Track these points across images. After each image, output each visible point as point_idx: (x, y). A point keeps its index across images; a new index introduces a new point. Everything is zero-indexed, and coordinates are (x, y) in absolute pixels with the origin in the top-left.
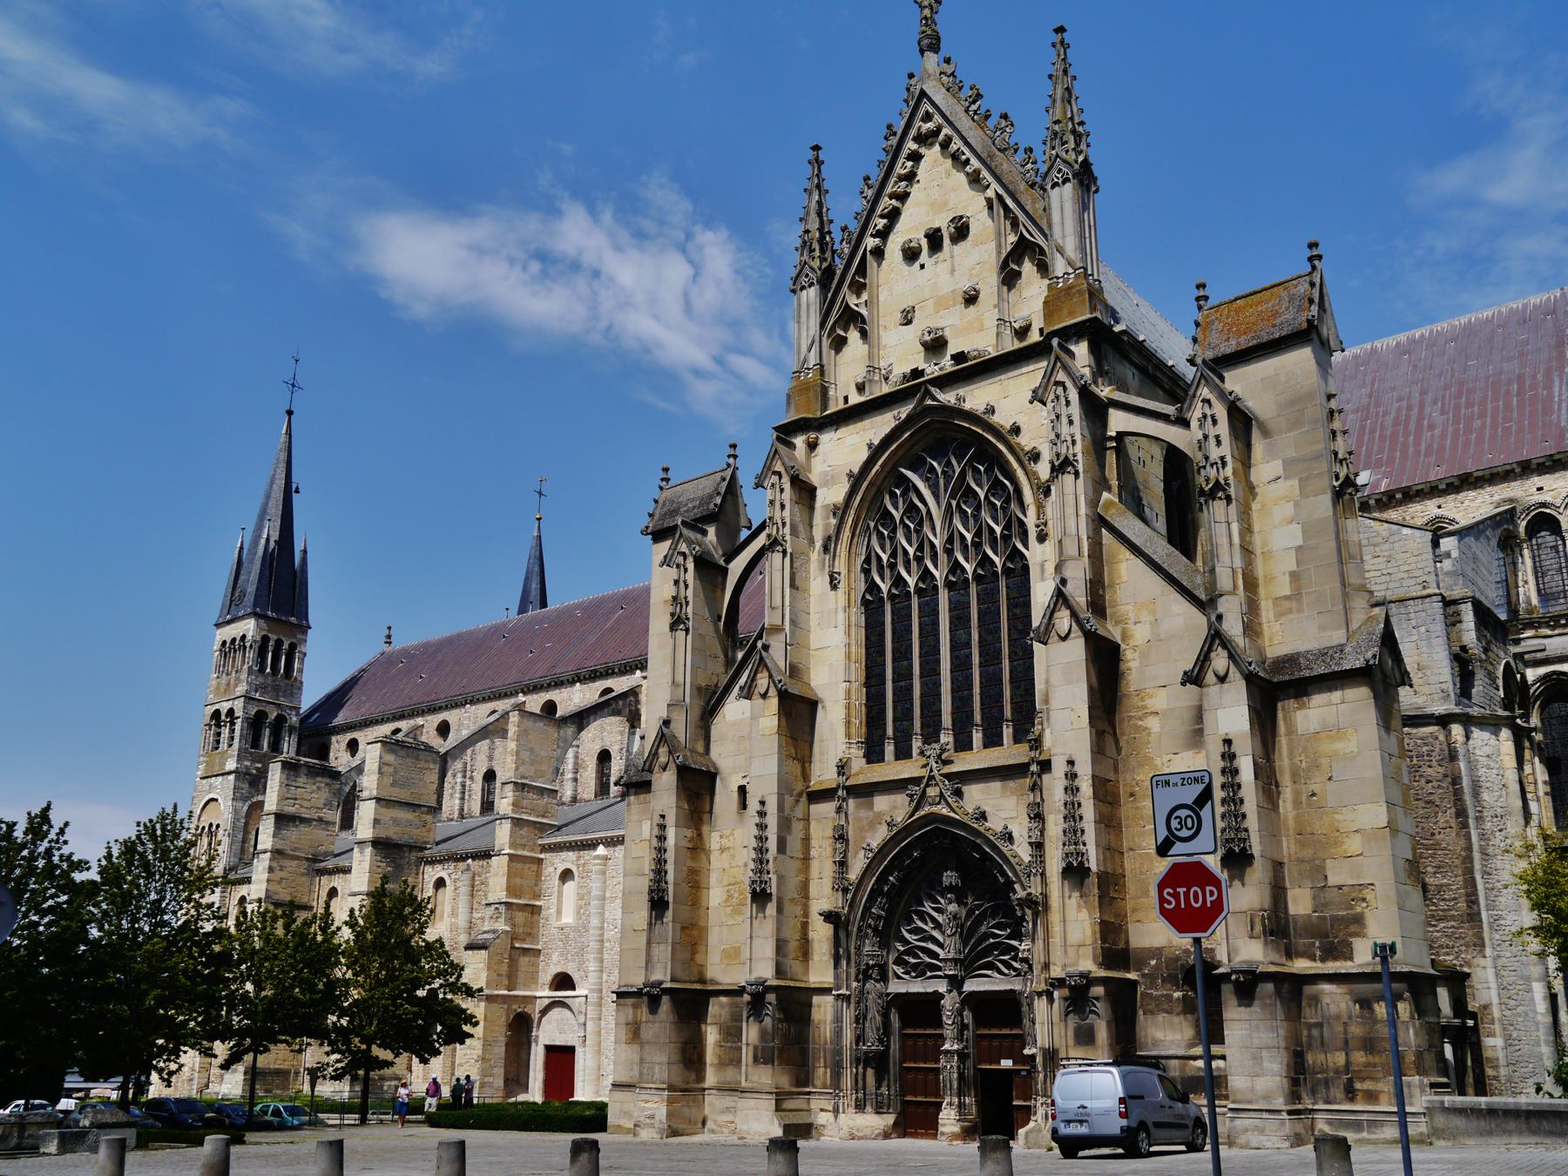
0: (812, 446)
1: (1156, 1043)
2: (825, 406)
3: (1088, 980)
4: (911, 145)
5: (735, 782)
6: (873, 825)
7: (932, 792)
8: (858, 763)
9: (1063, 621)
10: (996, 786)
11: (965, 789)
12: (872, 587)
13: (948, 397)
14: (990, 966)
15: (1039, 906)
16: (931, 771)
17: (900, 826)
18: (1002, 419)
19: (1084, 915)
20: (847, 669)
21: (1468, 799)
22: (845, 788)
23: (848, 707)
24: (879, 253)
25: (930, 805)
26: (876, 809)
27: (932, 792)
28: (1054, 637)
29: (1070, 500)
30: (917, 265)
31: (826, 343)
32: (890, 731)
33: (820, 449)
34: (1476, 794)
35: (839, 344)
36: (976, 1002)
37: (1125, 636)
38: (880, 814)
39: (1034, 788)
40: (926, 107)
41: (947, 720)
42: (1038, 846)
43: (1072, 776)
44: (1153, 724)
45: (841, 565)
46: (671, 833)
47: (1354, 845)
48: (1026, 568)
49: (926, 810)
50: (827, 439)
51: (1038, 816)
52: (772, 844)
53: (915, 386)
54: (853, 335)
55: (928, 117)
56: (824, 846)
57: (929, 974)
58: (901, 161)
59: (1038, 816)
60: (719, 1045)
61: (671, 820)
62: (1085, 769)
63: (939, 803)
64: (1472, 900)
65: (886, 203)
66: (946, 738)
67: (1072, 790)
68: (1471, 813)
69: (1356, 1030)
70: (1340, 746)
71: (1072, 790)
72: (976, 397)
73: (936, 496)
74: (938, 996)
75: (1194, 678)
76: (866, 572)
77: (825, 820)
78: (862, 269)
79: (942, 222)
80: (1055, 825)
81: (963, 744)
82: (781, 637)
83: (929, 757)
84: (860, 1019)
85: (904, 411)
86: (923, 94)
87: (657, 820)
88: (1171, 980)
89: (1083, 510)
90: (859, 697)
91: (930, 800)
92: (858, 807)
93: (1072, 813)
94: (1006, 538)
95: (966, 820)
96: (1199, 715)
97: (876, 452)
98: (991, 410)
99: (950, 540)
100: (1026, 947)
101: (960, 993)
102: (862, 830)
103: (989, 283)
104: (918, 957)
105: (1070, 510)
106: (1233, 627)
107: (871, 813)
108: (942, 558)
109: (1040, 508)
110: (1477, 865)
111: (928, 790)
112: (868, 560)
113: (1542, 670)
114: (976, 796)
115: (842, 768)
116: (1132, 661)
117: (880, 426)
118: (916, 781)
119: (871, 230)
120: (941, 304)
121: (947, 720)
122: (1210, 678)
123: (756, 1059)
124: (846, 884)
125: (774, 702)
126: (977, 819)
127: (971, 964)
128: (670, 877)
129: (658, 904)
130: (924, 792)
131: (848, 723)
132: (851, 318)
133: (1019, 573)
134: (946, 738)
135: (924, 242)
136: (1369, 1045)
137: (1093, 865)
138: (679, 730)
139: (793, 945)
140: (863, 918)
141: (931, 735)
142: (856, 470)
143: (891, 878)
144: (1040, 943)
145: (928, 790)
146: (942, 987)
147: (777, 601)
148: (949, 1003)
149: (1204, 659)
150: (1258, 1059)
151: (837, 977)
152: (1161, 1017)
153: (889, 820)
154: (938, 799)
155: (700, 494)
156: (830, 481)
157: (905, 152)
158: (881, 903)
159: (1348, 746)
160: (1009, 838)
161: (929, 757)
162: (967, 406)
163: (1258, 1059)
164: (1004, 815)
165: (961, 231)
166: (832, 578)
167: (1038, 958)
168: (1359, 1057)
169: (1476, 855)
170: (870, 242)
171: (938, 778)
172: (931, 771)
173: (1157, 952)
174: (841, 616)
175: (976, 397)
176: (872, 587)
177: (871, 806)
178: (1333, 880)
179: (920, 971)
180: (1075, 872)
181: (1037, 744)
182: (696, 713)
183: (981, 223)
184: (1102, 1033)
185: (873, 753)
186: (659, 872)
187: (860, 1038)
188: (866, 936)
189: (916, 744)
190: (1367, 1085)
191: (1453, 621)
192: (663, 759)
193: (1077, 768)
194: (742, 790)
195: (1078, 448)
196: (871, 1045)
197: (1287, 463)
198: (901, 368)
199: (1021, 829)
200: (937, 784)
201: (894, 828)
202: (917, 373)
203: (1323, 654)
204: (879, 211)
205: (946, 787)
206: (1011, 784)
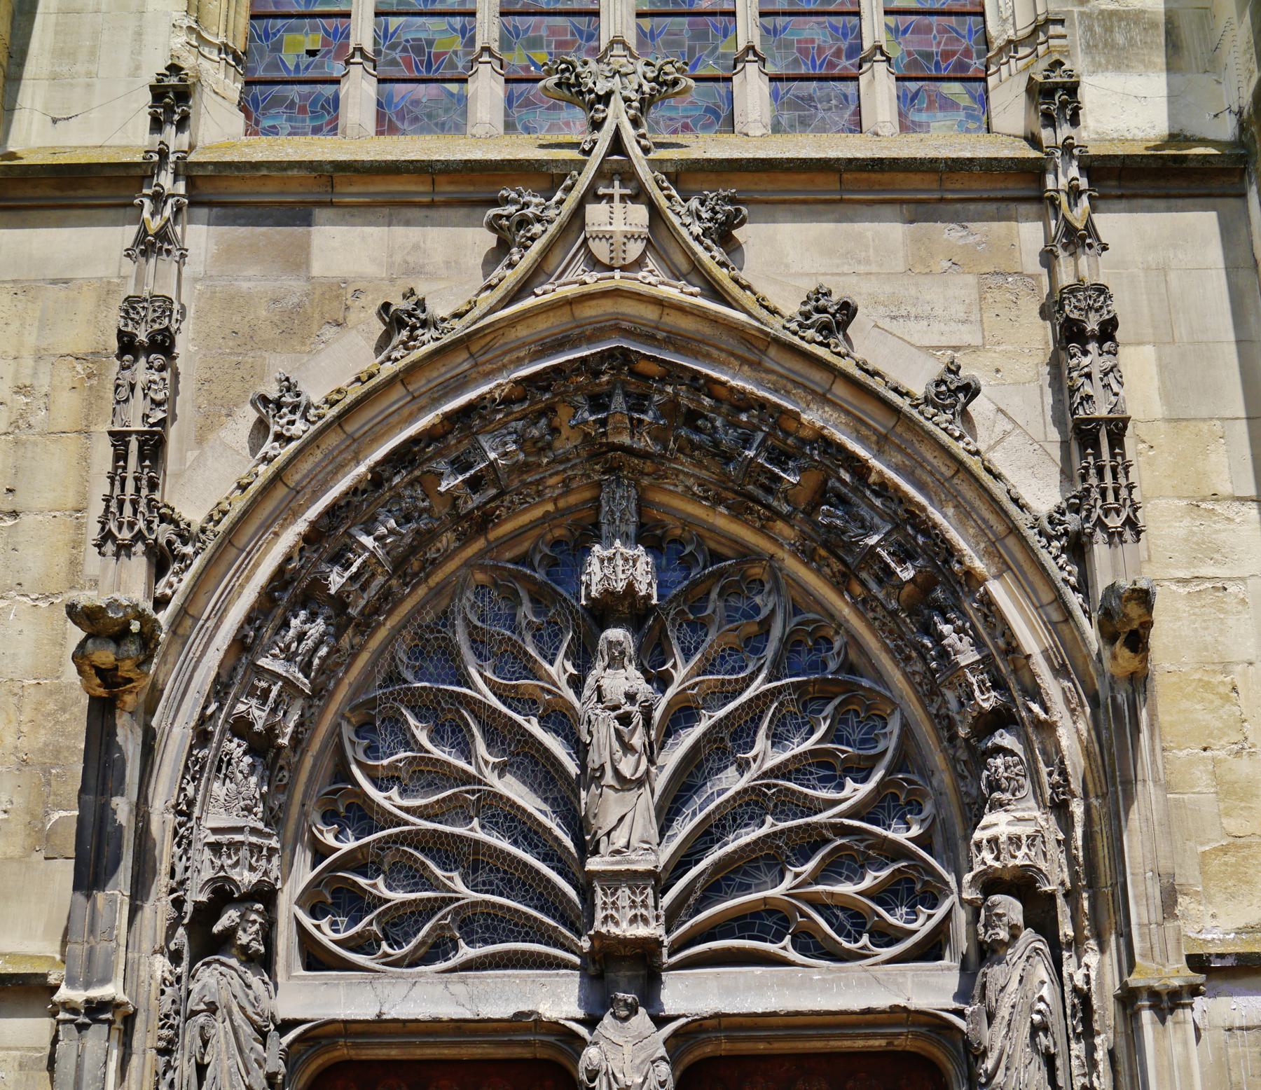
16: (617, 145)
17: (460, 328)
22: (188, 172)
25: (594, 263)
26: (317, 269)
56: (43, 383)
57: (467, 952)
63: (639, 264)
77: (57, 292)
83: (606, 99)
91: (601, 250)
92: (228, 253)
95: (775, 326)
100: (1024, 830)
101: (660, 1021)
102: (246, 339)
104: (421, 879)
107: (294, 286)
111: (596, 214)
124: (163, 533)
126: (824, 328)
130: (578, 214)
140: (220, 688)
143: (368, 541)
145: (596, 214)
153: (399, 304)
154: (635, 250)
158: (301, 637)
161: (606, 99)
164: (920, 333)
171: (645, 173)
172: (617, 145)
177: (298, 260)
188: (222, 765)
200: (639, 195)
201: (426, 334)
206: (948, 234)
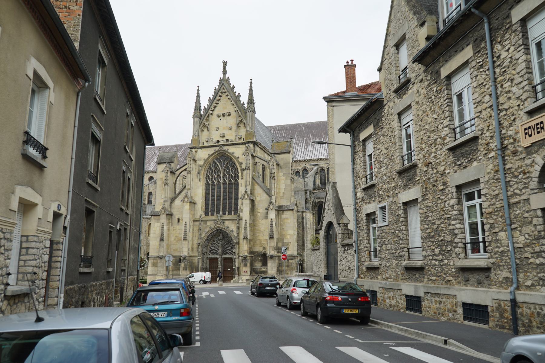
0: (196, 152)
1: (256, 266)
2: (199, 145)
3: (247, 256)
4: (220, 94)
5: (177, 217)
6: (206, 227)
7: (219, 222)
8: (203, 215)
9: (246, 196)
10: (231, 222)
11: (225, 222)
12: (208, 182)
13: (225, 148)
14: (226, 253)
15: (238, 243)
18: (236, 155)
19: (246, 246)
20: (202, 198)
21: (305, 225)
23: (202, 205)
24: (212, 114)
27: (219, 222)
28: (244, 199)
29: (248, 174)
30: (219, 119)
31: (200, 131)
32: (210, 210)
33: (198, 153)
34: (306, 225)
35: (203, 131)
36: (225, 259)
37: (255, 199)
38: (208, 226)
39: (238, 223)
40: (223, 87)
41: (221, 209)
42: (238, 233)
43: (246, 223)
44: (259, 214)
45: (202, 177)
46: (165, 228)
47: (288, 236)
48: (238, 184)
49: (217, 226)
50: (199, 151)
51: (238, 228)
52: (188, 230)
53: (217, 144)
54: (205, 130)
55: (224, 89)
58: (218, 97)
59: (238, 228)
60: (172, 267)
61: (165, 224)
62: (248, 222)
64: (303, 242)
65: (214, 105)
66: (221, 213)
67: (246, 225)
68: (305, 228)
69: (286, 264)
70: (288, 221)
71: (246, 225)
72: (231, 149)
73: (221, 166)
74: (217, 259)
75: (267, 209)
76: (206, 179)
78: (208, 116)
79: (225, 111)
80: (242, 231)
81: (224, 214)
82: (190, 191)
84: (203, 262)
85: (217, 148)
86: (223, 84)
87: (161, 224)
88: (259, 256)
89: (251, 177)
90: (204, 203)
93: (246, 229)
94: (235, 177)
96: (267, 213)
97: (210, 156)
98: (233, 153)
99: (224, 175)
103: (234, 127)
105: (248, 176)
106: (274, 201)
108: (222, 178)
109: (242, 173)
110: (305, 237)
112: (207, 176)
113: (319, 200)
114: (227, 223)
115: (200, 216)
116: (256, 203)
117: (211, 151)
118: (216, 220)
119: (210, 109)
120: (224, 128)
121: (221, 209)
122: (270, 209)
123: (183, 269)
125: (189, 204)
127: (224, 252)
128: (165, 235)
129: (162, 240)
131: (202, 208)
132: (205, 126)
133: (237, 184)
134: (221, 213)
135: (222, 115)
136: (288, 266)
137: (249, 238)
138: (167, 206)
139: (190, 249)
141: (218, 212)
142: (206, 159)
144: (237, 250)
146: (218, 257)
147: (189, 184)
148: (219, 259)
149: (269, 206)
150: (272, 268)
151: (199, 255)
152: (257, 262)
155: (169, 156)
156: (200, 160)
157: (219, 95)
159: (289, 221)
160: (233, 231)
162: (229, 151)
163: (272, 268)
165: (229, 115)
166: (200, 179)
167: (237, 252)
168: (286, 268)
169: (305, 235)
170: (211, 112)
173: (257, 252)
174: (201, 187)
175: (231, 149)
176: (208, 182)
178: (285, 242)
179: (214, 253)
180: (245, 238)
181: (239, 215)
182: (169, 202)
183: (234, 114)
184: (249, 265)
185: (206, 214)
186: (162, 234)
187: (203, 265)
189: (215, 213)
190: (287, 272)
191: (306, 193)
192: (163, 212)
193: (247, 222)
194: (179, 219)
195: (251, 165)
196: (204, 267)
197: (284, 174)
198: (215, 139)
199: (235, 230)
202: (218, 141)
203: (287, 206)
204: (213, 106)
205: (222, 222)
